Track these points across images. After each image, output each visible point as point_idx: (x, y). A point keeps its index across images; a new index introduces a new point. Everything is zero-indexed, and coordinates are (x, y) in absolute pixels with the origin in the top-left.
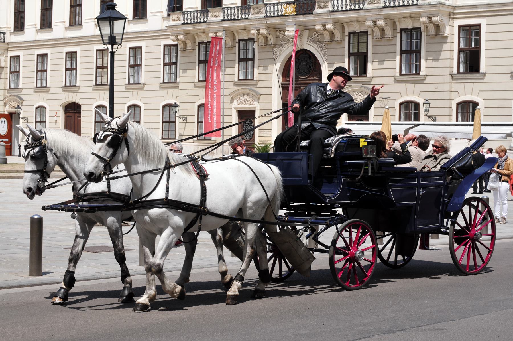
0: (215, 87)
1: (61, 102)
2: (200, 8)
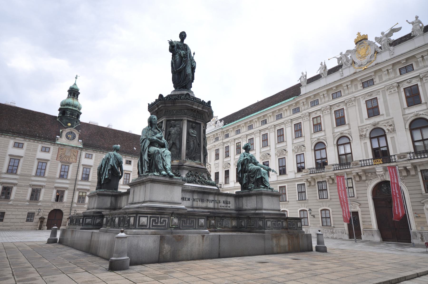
2: (315, 167)
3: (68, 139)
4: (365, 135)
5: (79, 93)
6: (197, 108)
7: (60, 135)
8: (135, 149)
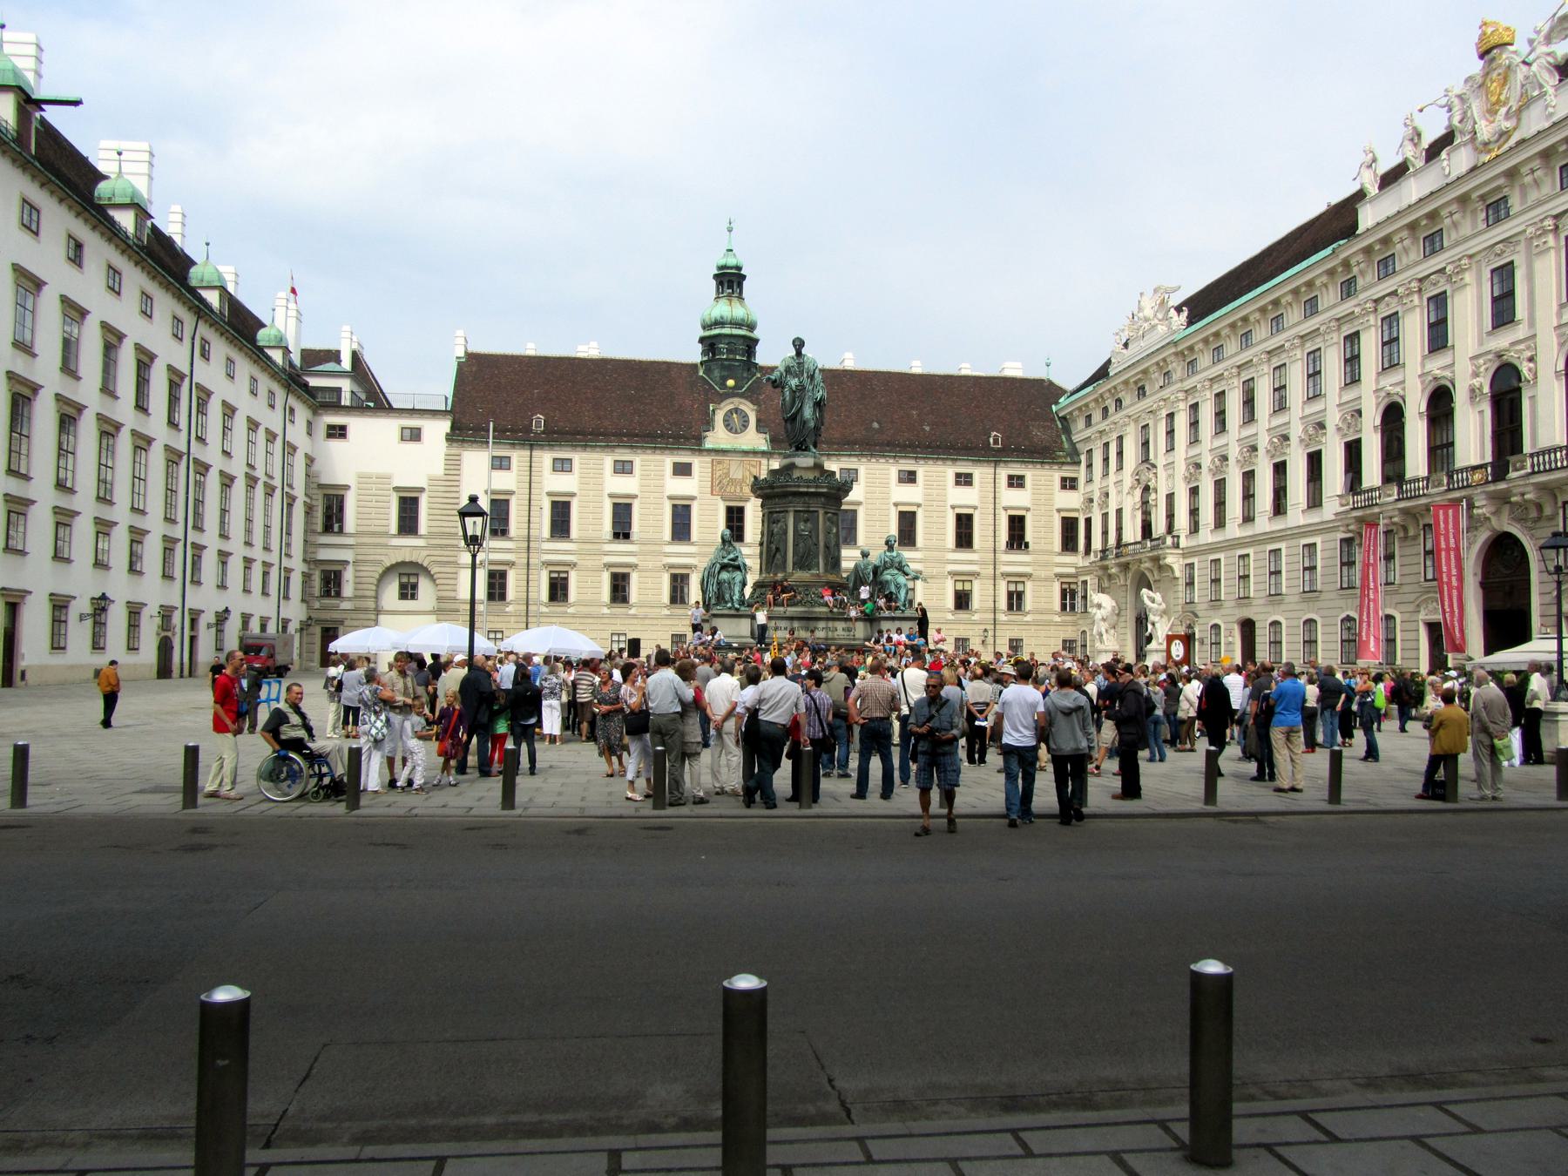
0: (1371, 592)
1: (1235, 619)
3: (730, 431)
4: (1480, 389)
5: (744, 277)
6: (805, 490)
7: (708, 424)
8: (927, 428)
